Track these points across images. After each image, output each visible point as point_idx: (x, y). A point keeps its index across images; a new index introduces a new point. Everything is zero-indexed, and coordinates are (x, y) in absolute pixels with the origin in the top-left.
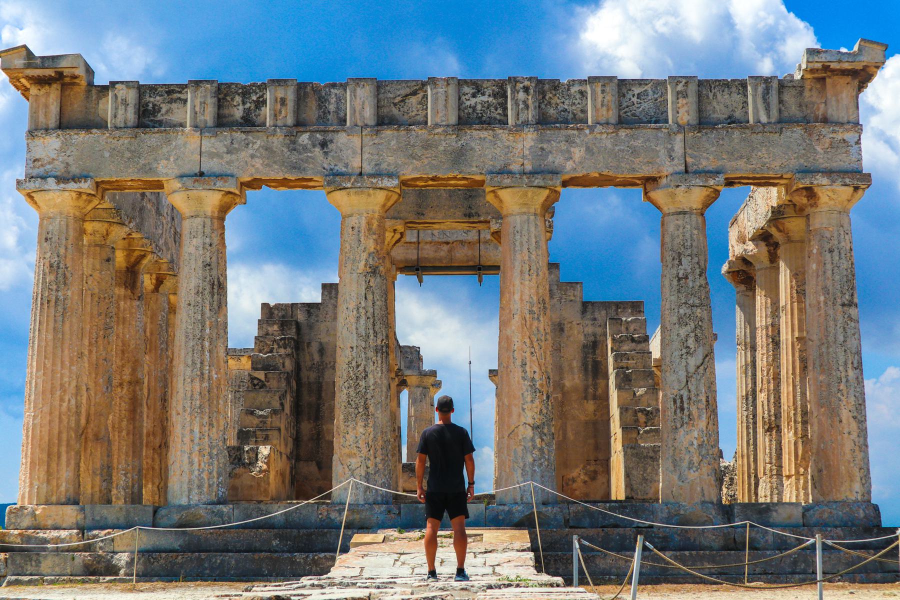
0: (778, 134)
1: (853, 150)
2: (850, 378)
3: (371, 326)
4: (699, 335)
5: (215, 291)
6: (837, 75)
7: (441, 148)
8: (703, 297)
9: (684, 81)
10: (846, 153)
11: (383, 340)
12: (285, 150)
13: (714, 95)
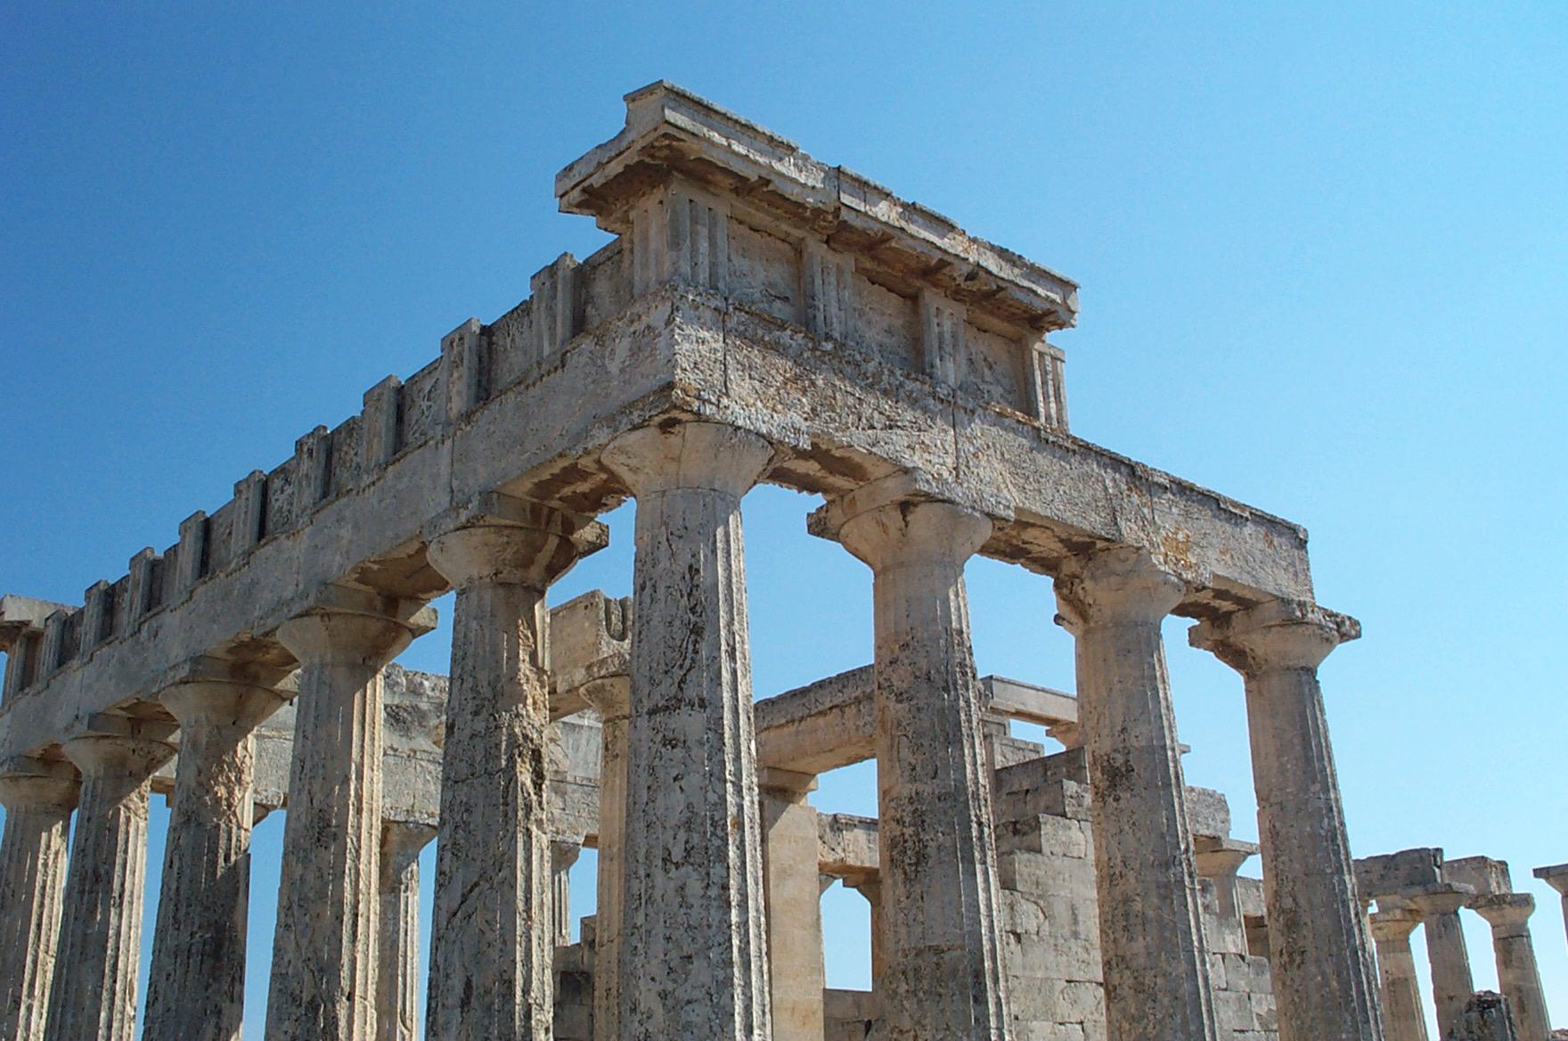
0: (560, 370)
1: (662, 342)
2: (657, 894)
3: (171, 915)
4: (462, 841)
5: (87, 888)
6: (644, 195)
7: (236, 592)
8: (478, 759)
9: (457, 336)
10: (651, 355)
11: (192, 935)
12: (130, 655)
13: (513, 340)
